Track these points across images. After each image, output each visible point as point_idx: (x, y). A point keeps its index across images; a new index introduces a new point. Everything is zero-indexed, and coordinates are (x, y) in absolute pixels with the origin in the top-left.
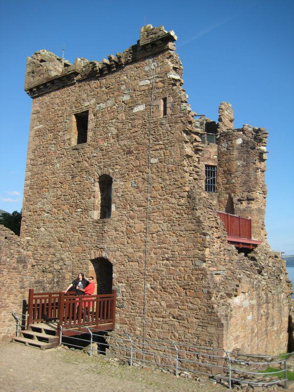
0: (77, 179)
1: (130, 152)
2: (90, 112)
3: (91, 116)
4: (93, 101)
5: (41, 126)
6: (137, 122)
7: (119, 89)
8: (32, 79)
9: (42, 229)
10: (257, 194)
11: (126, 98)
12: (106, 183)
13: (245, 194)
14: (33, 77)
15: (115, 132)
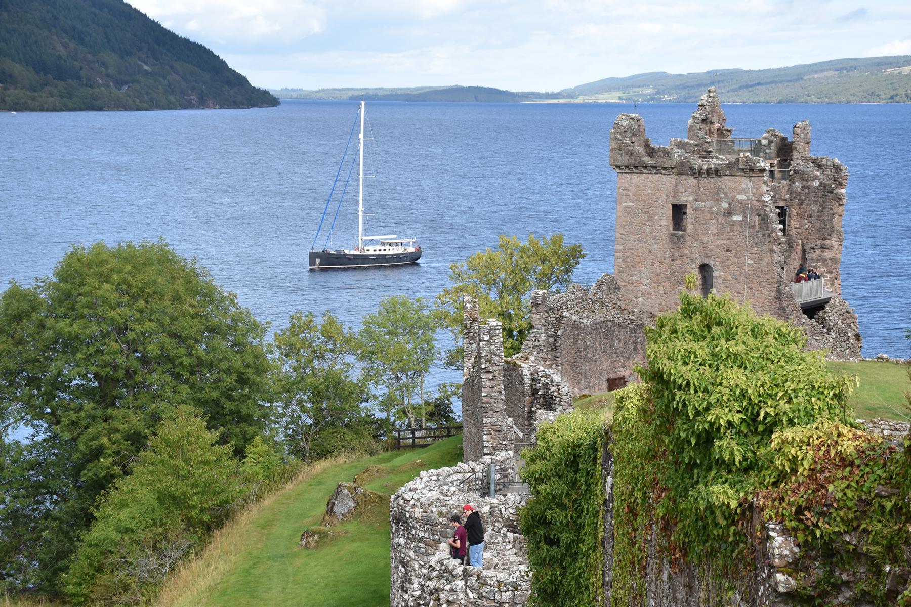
0: (678, 262)
1: (728, 251)
2: (689, 205)
3: (689, 211)
4: (691, 198)
5: (631, 204)
6: (735, 228)
7: (717, 194)
8: (619, 157)
9: (641, 299)
10: (833, 242)
11: (725, 205)
12: (705, 269)
13: (819, 242)
14: (621, 155)
15: (715, 231)
